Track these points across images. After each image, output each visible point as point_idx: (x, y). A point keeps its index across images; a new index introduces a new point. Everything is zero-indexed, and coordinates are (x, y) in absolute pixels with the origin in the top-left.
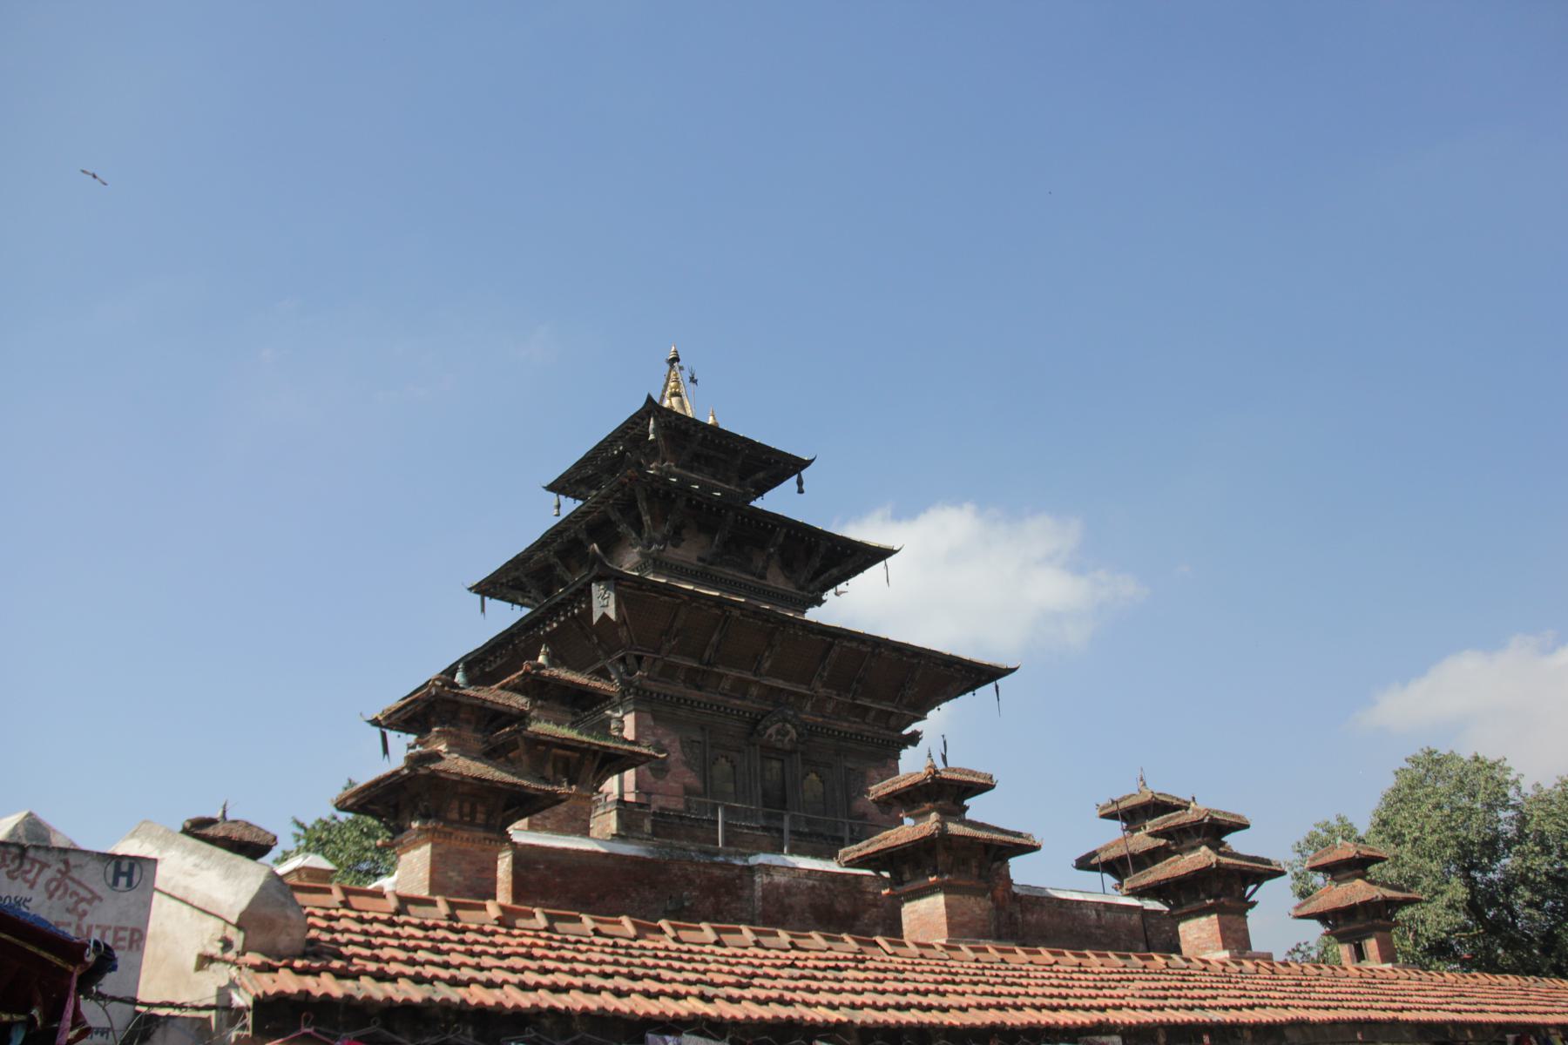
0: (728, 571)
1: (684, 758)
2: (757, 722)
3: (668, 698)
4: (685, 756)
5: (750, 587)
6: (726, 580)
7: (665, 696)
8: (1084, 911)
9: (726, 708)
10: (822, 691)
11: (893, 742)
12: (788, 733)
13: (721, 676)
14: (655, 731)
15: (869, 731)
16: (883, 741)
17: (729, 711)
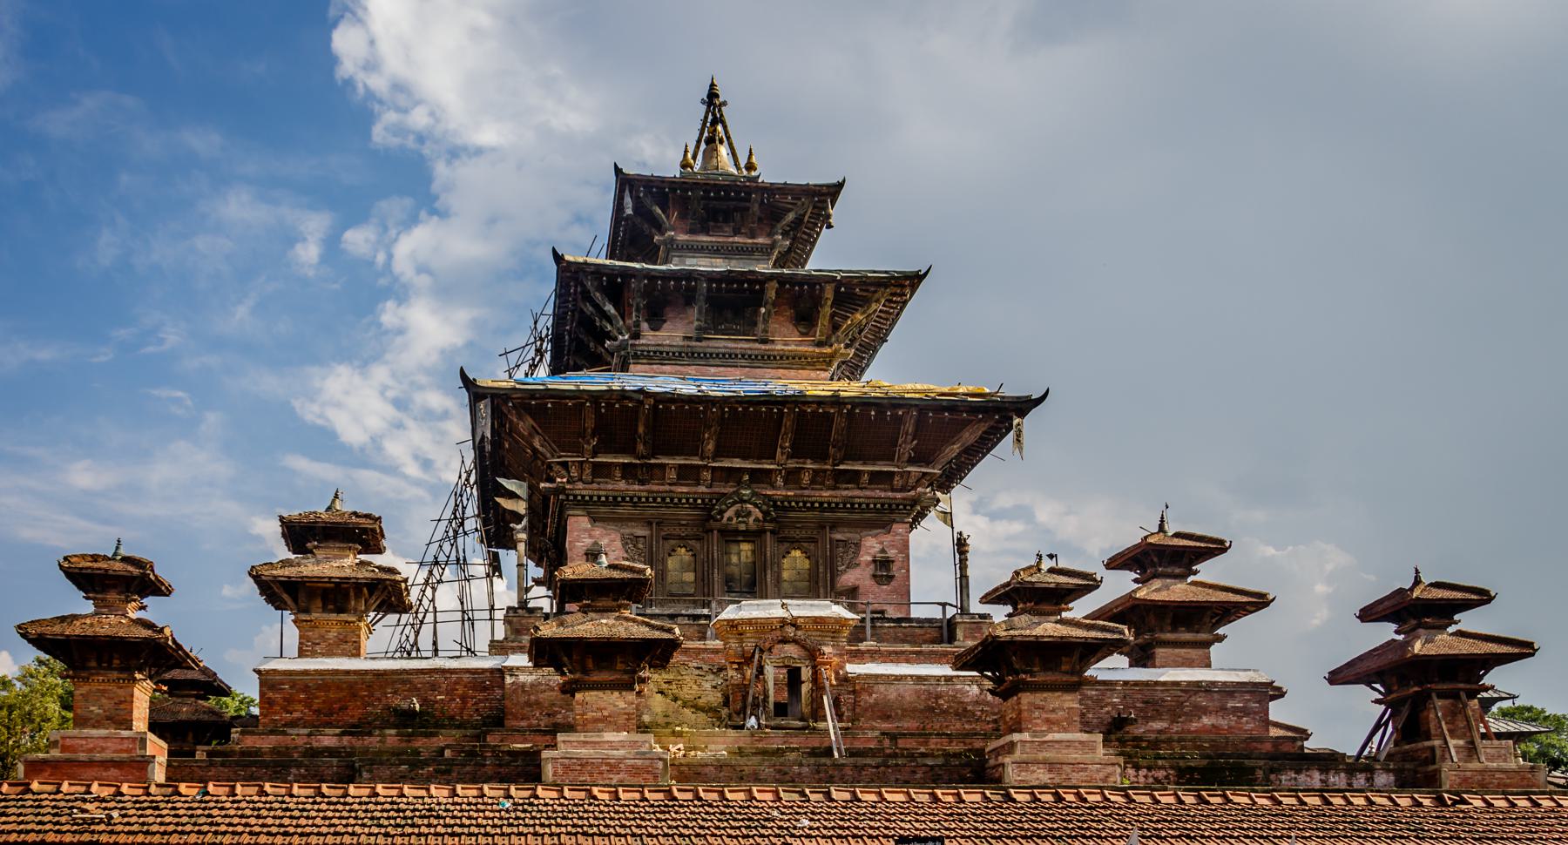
0: (722, 344)
1: (625, 555)
2: (715, 505)
3: (603, 499)
4: (627, 552)
5: (750, 356)
6: (717, 355)
7: (599, 497)
8: (959, 687)
9: (672, 499)
10: (792, 464)
11: (898, 505)
12: (749, 514)
13: (663, 466)
14: (593, 533)
15: (860, 498)
16: (883, 505)
17: (676, 500)
